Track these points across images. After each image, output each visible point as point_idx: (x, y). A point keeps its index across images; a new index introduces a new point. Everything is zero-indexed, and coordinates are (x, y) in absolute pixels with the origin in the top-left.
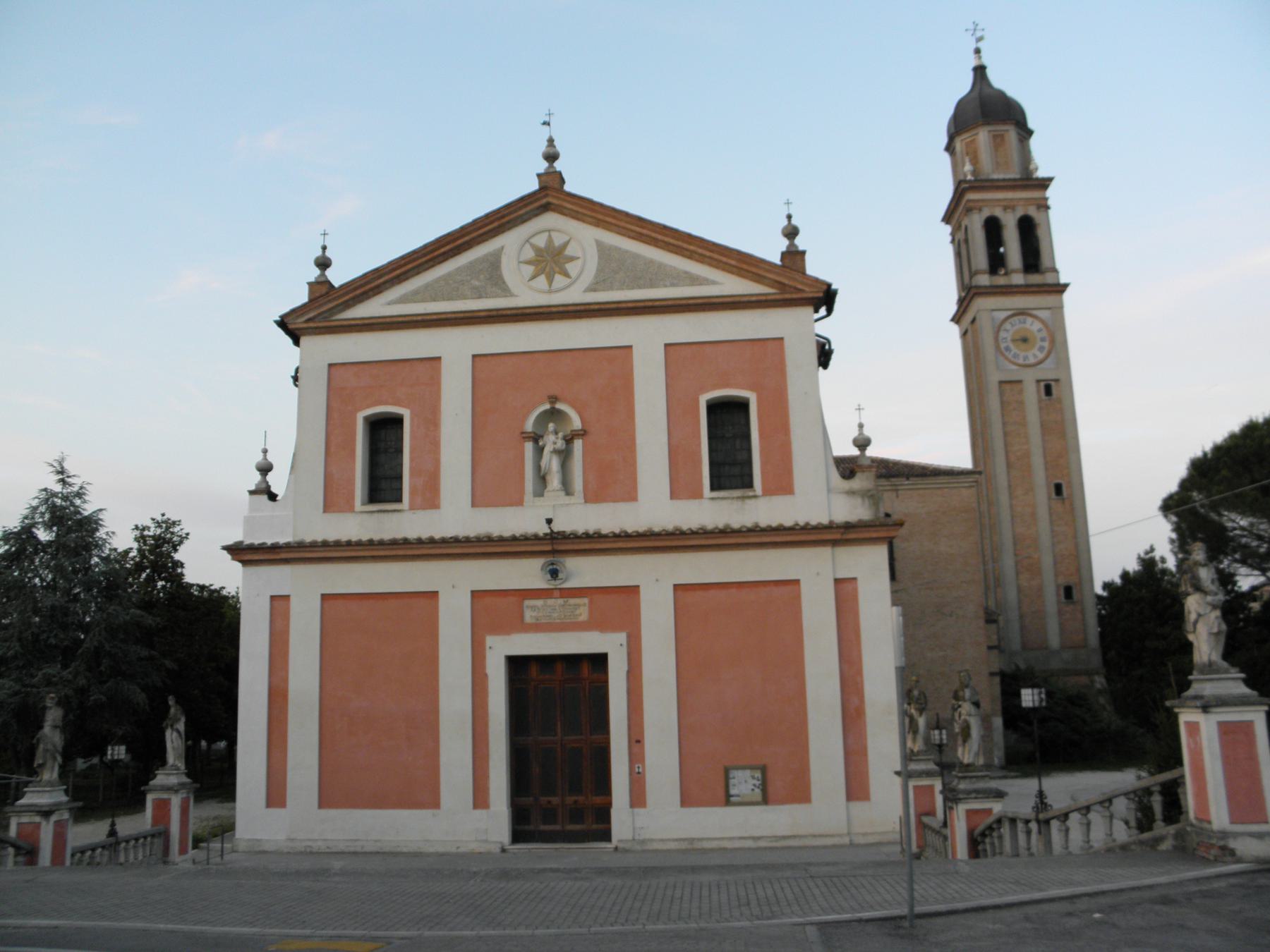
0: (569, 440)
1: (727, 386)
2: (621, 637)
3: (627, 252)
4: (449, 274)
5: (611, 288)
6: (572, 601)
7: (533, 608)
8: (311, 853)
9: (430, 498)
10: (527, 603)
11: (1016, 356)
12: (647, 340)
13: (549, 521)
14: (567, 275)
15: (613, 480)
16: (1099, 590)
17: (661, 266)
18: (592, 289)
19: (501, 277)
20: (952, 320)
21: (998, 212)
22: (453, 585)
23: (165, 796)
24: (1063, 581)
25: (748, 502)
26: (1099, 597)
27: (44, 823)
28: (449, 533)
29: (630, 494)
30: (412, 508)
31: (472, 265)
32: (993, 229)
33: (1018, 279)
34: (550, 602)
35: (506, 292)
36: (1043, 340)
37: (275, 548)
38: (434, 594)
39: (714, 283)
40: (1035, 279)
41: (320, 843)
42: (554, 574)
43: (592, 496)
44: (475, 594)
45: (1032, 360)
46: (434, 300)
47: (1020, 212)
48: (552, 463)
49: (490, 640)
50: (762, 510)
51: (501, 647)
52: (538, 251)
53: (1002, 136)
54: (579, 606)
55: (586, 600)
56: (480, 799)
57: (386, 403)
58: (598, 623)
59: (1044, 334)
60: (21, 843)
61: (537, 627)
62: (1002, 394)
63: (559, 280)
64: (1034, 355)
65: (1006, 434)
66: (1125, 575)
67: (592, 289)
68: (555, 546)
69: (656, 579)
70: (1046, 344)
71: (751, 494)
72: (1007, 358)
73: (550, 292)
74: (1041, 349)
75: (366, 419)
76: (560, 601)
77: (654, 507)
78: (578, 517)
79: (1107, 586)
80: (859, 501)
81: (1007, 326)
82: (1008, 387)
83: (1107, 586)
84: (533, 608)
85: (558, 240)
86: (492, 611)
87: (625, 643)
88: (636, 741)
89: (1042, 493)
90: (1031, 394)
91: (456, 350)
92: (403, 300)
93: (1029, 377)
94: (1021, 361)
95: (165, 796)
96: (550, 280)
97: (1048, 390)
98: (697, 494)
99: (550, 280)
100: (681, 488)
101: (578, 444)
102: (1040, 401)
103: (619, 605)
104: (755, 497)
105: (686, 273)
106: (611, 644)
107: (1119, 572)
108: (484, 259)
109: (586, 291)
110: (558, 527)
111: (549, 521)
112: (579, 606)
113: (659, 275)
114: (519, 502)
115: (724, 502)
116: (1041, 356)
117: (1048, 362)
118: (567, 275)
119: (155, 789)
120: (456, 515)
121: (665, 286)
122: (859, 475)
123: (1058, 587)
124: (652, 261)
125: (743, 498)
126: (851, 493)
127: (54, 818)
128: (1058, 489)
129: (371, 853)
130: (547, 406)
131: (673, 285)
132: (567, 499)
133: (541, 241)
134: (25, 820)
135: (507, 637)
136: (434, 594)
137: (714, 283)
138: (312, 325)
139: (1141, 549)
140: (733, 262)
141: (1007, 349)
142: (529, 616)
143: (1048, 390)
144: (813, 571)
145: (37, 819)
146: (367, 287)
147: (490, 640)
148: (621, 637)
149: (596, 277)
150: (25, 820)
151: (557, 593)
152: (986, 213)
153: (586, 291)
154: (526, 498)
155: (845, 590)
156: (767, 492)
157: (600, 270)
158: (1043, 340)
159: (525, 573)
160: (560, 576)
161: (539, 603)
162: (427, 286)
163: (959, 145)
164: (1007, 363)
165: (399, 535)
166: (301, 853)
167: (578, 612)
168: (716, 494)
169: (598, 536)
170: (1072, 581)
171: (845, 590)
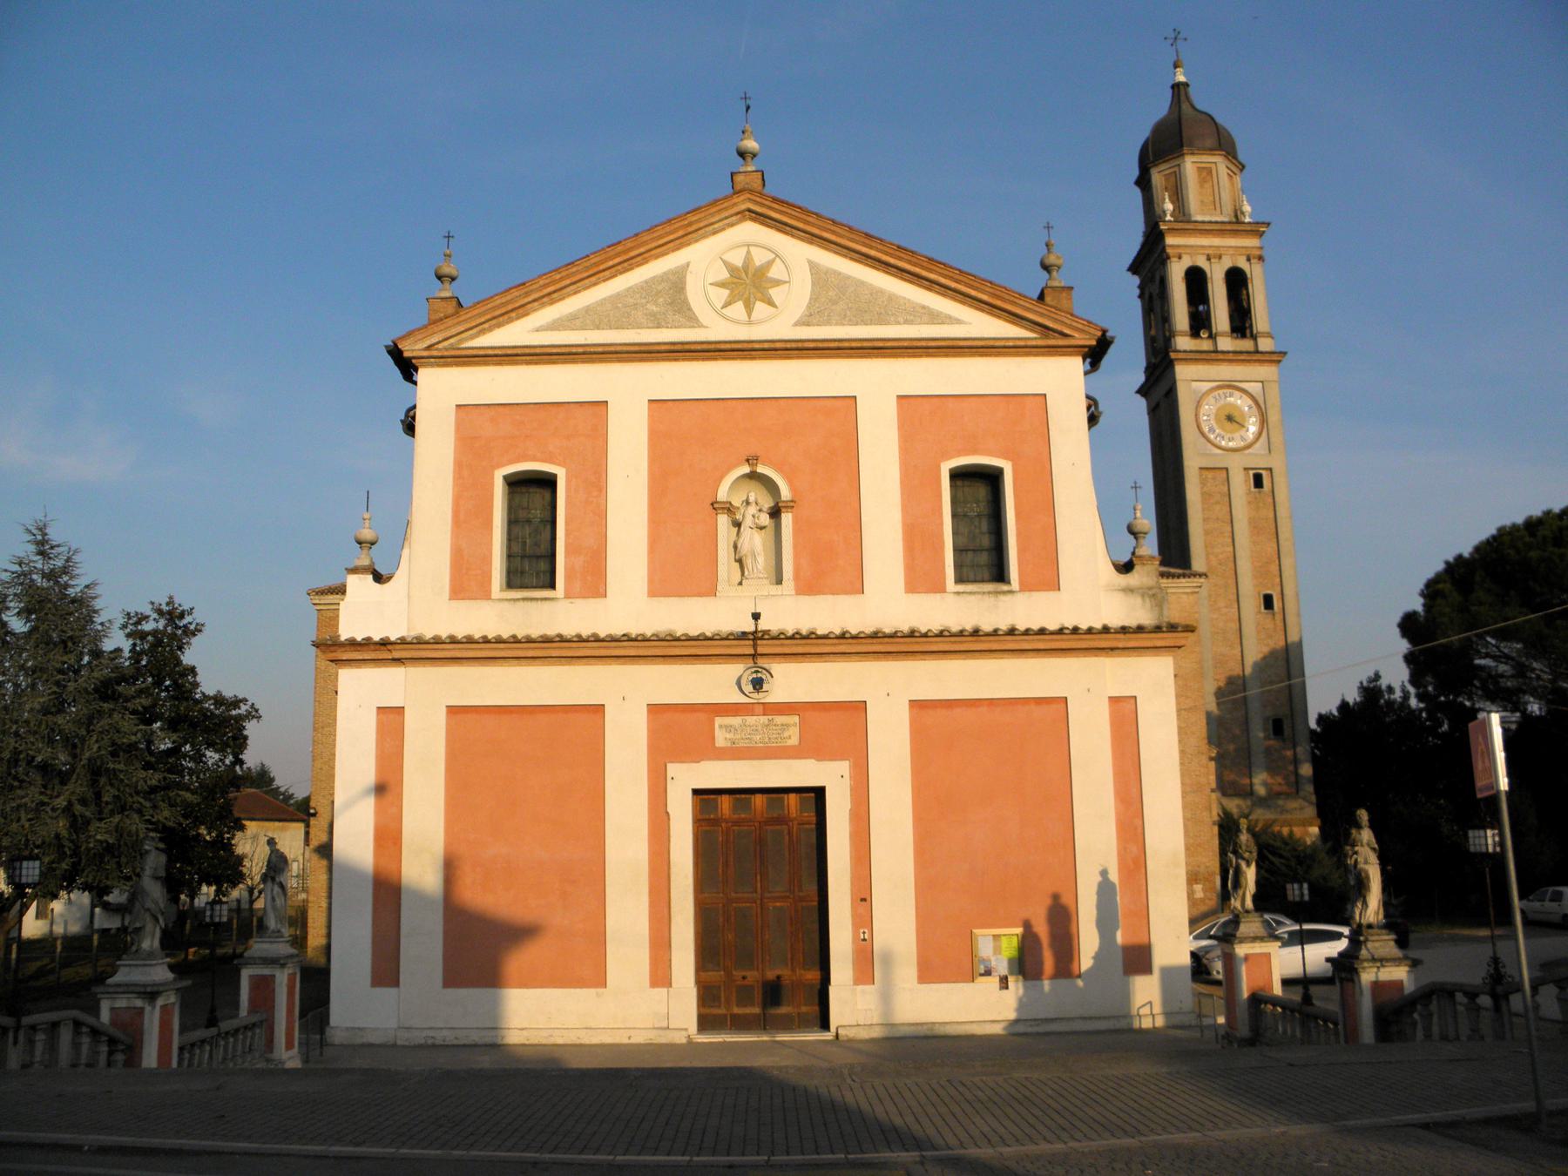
0: (775, 513)
1: (975, 452)
2: (843, 767)
3: (849, 277)
4: (618, 296)
5: (828, 323)
6: (780, 719)
7: (728, 728)
8: (434, 1046)
9: (594, 583)
10: (718, 721)
12: (875, 387)
13: (756, 616)
14: (771, 303)
15: (833, 567)
16: (1313, 725)
17: (892, 298)
18: (800, 323)
19: (685, 302)
20: (1139, 392)
21: (1201, 262)
22: (627, 697)
23: (266, 971)
25: (1002, 597)
26: (1313, 732)
27: (148, 1009)
28: (618, 631)
29: (856, 586)
30: (567, 596)
31: (647, 288)
32: (1196, 278)
33: (1226, 343)
34: (751, 720)
35: (693, 321)
37: (385, 643)
38: (599, 709)
39: (959, 322)
41: (445, 1033)
42: (758, 684)
43: (809, 586)
44: (655, 710)
46: (598, 328)
47: (1227, 263)
48: (755, 542)
49: (673, 769)
50: (1017, 608)
51: (686, 778)
52: (732, 269)
53: (1210, 171)
54: (786, 726)
55: (796, 719)
56: (661, 976)
57: (534, 459)
58: (810, 749)
60: (118, 1034)
61: (735, 753)
62: (1203, 483)
63: (760, 308)
65: (1207, 533)
66: (1344, 706)
67: (800, 323)
68: (755, 647)
69: (889, 692)
71: (1005, 588)
72: (1209, 441)
73: (750, 323)
75: (506, 478)
76: (764, 719)
77: (886, 602)
78: (789, 612)
79: (1321, 719)
80: (1139, 600)
81: (1210, 399)
82: (1210, 475)
84: (728, 728)
85: (760, 257)
86: (677, 730)
87: (847, 775)
88: (863, 899)
90: (1240, 485)
91: (628, 392)
92: (554, 326)
93: (1236, 465)
95: (266, 971)
96: (749, 309)
98: (940, 589)
99: (749, 309)
100: (920, 579)
101: (787, 519)
102: (1250, 492)
103: (840, 727)
104: (1011, 592)
105: (924, 307)
106: (832, 776)
107: (1337, 702)
108: (664, 278)
109: (796, 324)
110: (764, 625)
111: (756, 616)
112: (788, 725)
113: (887, 309)
114: (711, 591)
115: (972, 598)
117: (1257, 445)
118: (771, 303)
119: (253, 961)
120: (628, 605)
121: (898, 323)
122: (1137, 568)
124: (881, 292)
125: (997, 593)
126: (1128, 590)
127: (160, 1002)
128: (1268, 602)
129: (464, 1046)
130: (746, 469)
131: (906, 322)
132: (775, 589)
133: (737, 259)
134: (121, 1003)
135: (694, 765)
136: (599, 709)
137: (959, 322)
138: (435, 353)
139: (1364, 675)
140: (985, 297)
142: (721, 739)
144: (1085, 685)
145: (139, 1003)
146: (510, 307)
147: (673, 769)
148: (843, 767)
149: (809, 306)
150: (121, 1003)
151: (760, 709)
152: (1187, 262)
153: (796, 324)
154: (721, 586)
155: (1124, 713)
156: (1026, 587)
157: (814, 299)
159: (716, 682)
160: (765, 687)
161: (735, 721)
162: (587, 310)
163: (1157, 177)
165: (551, 632)
166: (420, 1046)
167: (786, 734)
168: (961, 588)
169: (811, 636)
171: (1124, 713)
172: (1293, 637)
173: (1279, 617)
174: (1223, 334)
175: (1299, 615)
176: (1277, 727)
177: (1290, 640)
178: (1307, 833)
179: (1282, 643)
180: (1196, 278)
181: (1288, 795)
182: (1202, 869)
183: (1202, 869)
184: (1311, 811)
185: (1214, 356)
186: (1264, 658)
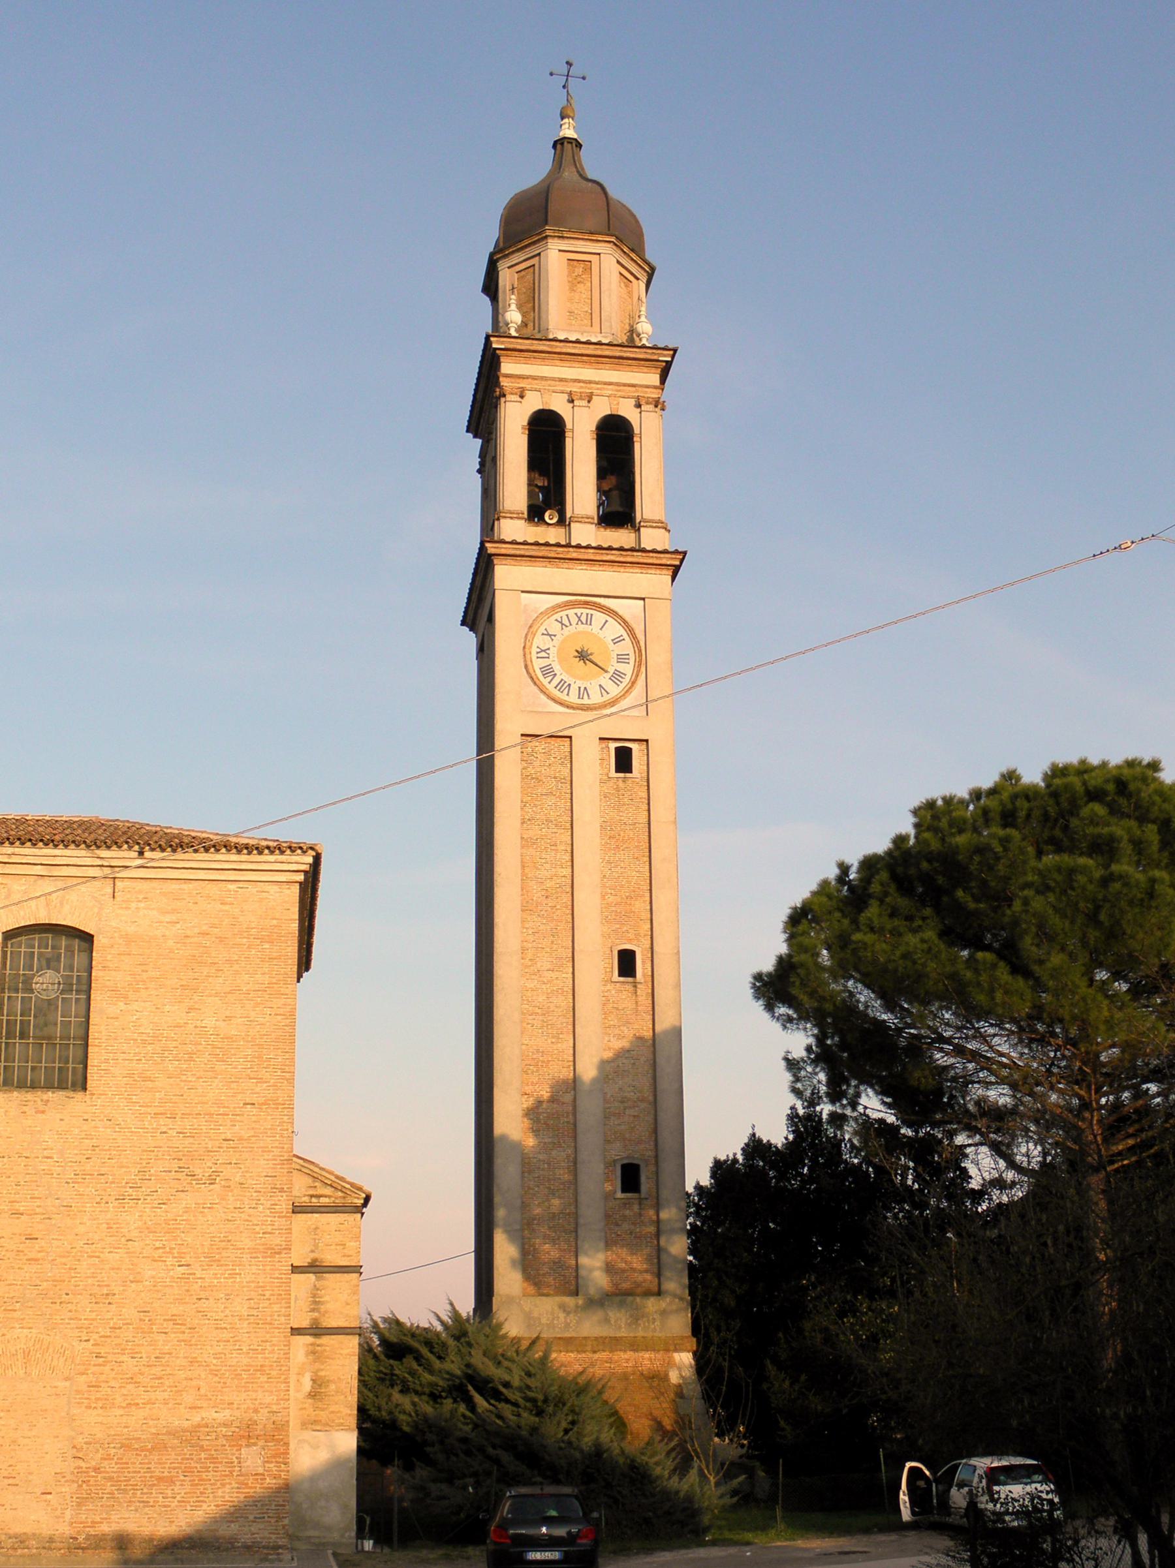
11: (563, 686)
20: (463, 623)
21: (558, 405)
24: (619, 1153)
32: (547, 433)
33: (586, 533)
36: (622, 659)
40: (621, 537)
45: (596, 698)
47: (601, 408)
59: (627, 647)
62: (526, 760)
64: (598, 687)
65: (526, 842)
66: (755, 1147)
70: (628, 669)
74: (617, 676)
79: (719, 1169)
82: (539, 746)
83: (719, 1169)
89: (597, 966)
94: (573, 698)
97: (624, 761)
116: (614, 690)
123: (610, 1164)
128: (626, 963)
141: (548, 671)
143: (624, 761)
152: (534, 403)
158: (622, 659)
163: (506, 276)
164: (543, 697)
170: (640, 1153)
172: (664, 1023)
173: (643, 991)
174: (581, 520)
175: (678, 985)
176: (630, 1177)
177: (658, 1029)
178: (671, 1363)
179: (648, 1034)
180: (547, 433)
181: (648, 1294)
182: (262, 1416)
183: (262, 1416)
184: (679, 1323)
185: (565, 554)
186: (622, 1054)
